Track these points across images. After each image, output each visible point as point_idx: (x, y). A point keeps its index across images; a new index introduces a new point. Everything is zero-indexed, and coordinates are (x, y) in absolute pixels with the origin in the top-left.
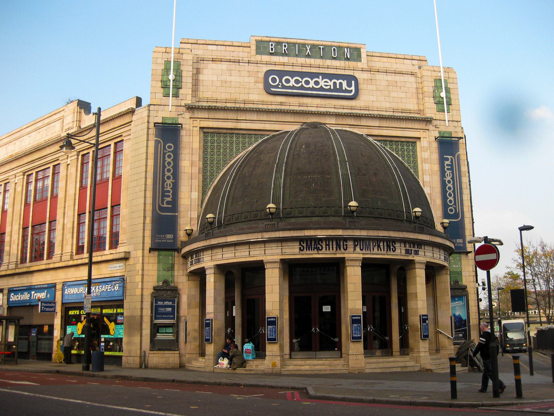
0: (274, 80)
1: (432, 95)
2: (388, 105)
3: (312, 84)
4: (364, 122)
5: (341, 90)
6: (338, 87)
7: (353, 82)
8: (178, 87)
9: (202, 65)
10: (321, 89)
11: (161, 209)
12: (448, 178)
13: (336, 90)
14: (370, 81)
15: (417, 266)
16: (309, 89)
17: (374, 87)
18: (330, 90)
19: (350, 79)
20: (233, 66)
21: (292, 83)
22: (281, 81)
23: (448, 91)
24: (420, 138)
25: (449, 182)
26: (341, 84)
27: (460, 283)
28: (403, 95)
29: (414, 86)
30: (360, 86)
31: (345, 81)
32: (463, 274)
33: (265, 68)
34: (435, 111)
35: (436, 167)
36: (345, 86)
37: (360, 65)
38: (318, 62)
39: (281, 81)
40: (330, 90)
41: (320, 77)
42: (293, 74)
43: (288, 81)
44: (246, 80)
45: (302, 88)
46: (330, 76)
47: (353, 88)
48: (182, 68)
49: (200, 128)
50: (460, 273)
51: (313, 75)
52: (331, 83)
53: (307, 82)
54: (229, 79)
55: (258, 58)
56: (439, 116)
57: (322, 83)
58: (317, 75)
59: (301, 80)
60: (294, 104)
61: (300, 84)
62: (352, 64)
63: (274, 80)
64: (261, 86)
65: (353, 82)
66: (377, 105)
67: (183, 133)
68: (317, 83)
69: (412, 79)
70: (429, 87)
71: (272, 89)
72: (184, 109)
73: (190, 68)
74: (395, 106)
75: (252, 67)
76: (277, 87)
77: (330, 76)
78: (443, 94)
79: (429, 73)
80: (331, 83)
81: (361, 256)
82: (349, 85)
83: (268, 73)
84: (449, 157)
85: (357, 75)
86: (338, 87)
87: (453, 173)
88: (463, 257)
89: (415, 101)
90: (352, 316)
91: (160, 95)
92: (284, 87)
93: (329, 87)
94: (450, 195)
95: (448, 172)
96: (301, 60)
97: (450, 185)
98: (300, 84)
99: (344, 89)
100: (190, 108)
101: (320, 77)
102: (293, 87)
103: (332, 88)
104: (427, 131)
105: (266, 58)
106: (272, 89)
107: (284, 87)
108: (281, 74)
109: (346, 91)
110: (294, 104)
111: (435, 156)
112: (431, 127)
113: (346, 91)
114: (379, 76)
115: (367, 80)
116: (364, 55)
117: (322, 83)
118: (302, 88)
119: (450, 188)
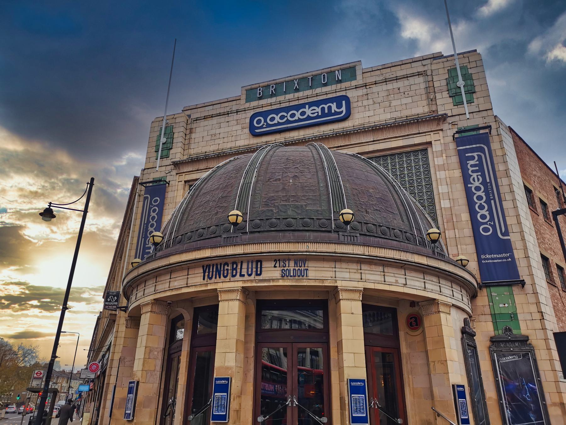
1: (445, 88)
2: (388, 116)
3: (298, 115)
4: (354, 140)
5: (330, 113)
6: (326, 111)
7: (344, 102)
8: (168, 147)
9: (194, 126)
10: (309, 118)
13: (324, 115)
14: (365, 97)
15: (342, 295)
16: (295, 121)
17: (371, 102)
20: (222, 119)
21: (277, 119)
22: (266, 121)
23: (467, 77)
24: (430, 143)
26: (330, 108)
27: (515, 332)
28: (409, 100)
29: (423, 86)
30: (353, 105)
31: (335, 104)
32: (520, 317)
33: (250, 113)
34: (451, 106)
35: (458, 173)
37: (354, 83)
38: (308, 92)
39: (266, 121)
41: (307, 106)
42: (276, 111)
43: (272, 119)
44: (235, 128)
46: (317, 104)
47: (344, 109)
48: (174, 130)
49: (185, 182)
50: (514, 317)
51: (297, 108)
52: (319, 110)
53: (293, 115)
54: (218, 131)
55: (247, 105)
56: (457, 110)
57: (309, 111)
58: (303, 106)
59: (285, 114)
61: (286, 119)
63: (259, 122)
64: (247, 131)
65: (344, 102)
67: (169, 189)
68: (303, 113)
69: (421, 79)
70: (440, 82)
71: (256, 131)
72: (173, 166)
73: (182, 129)
74: (396, 115)
75: (241, 115)
77: (317, 104)
78: (461, 83)
79: (441, 65)
80: (319, 110)
81: (241, 284)
82: (339, 106)
85: (350, 94)
86: (326, 111)
87: (483, 176)
88: (516, 290)
89: (425, 103)
90: (351, 381)
91: (153, 159)
92: (269, 126)
93: (316, 114)
98: (286, 119)
99: (333, 111)
100: (176, 165)
101: (307, 106)
102: (279, 124)
103: (320, 114)
104: (441, 132)
105: (254, 104)
106: (256, 131)
107: (269, 126)
108: (265, 114)
111: (454, 160)
112: (445, 126)
113: (336, 113)
114: (375, 89)
115: (363, 96)
116: (359, 73)
117: (309, 111)
118: (288, 122)
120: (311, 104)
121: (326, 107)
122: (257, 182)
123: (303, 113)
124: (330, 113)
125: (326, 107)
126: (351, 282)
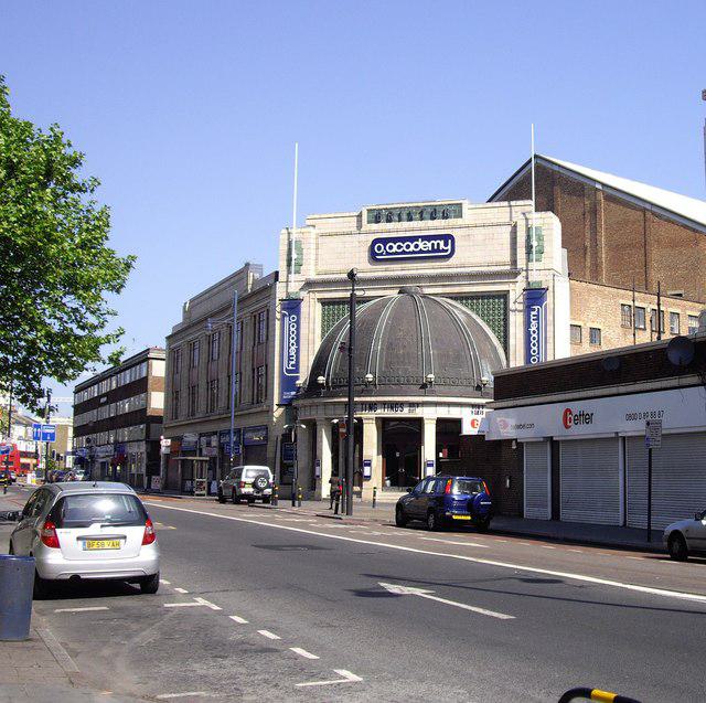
0: (379, 248)
3: (412, 248)
10: (421, 251)
11: (287, 370)
12: (533, 328)
13: (433, 251)
15: (426, 421)
16: (410, 253)
18: (428, 252)
19: (448, 238)
21: (395, 249)
25: (534, 332)
33: (372, 237)
36: (442, 246)
37: (459, 221)
40: (428, 252)
42: (395, 240)
43: (391, 248)
45: (404, 253)
47: (449, 247)
48: (303, 246)
52: (429, 245)
53: (408, 247)
60: (396, 270)
62: (452, 221)
63: (379, 248)
66: (473, 261)
76: (381, 254)
80: (429, 245)
82: (446, 245)
83: (376, 241)
84: (536, 307)
85: (455, 233)
92: (388, 254)
94: (534, 345)
95: (534, 322)
96: (405, 224)
97: (535, 335)
102: (396, 253)
105: (374, 227)
107: (388, 254)
108: (385, 241)
109: (444, 251)
110: (396, 270)
113: (444, 251)
117: (421, 245)
118: (404, 253)
119: (534, 339)
120: (425, 238)
121: (436, 243)
122: (382, 348)
123: (417, 246)
124: (438, 250)
125: (436, 243)
126: (430, 416)
